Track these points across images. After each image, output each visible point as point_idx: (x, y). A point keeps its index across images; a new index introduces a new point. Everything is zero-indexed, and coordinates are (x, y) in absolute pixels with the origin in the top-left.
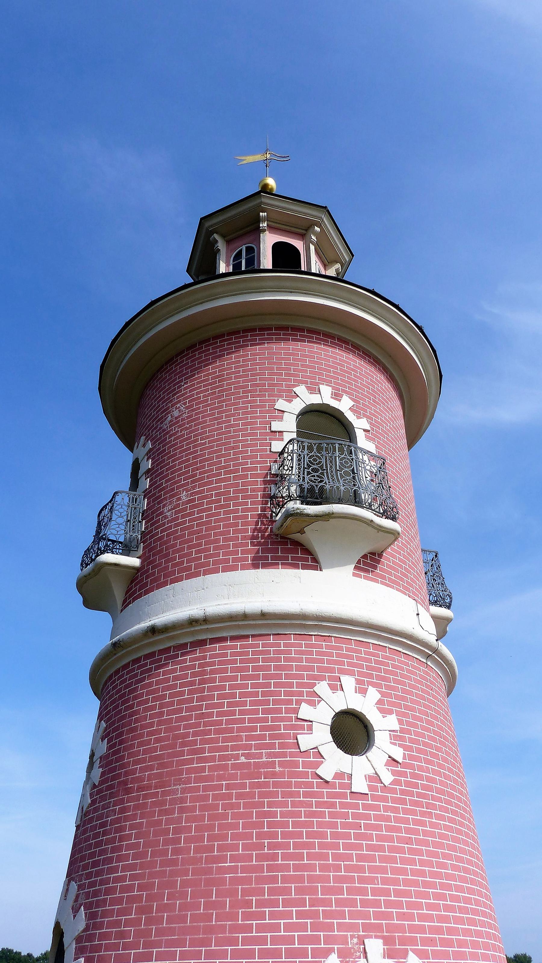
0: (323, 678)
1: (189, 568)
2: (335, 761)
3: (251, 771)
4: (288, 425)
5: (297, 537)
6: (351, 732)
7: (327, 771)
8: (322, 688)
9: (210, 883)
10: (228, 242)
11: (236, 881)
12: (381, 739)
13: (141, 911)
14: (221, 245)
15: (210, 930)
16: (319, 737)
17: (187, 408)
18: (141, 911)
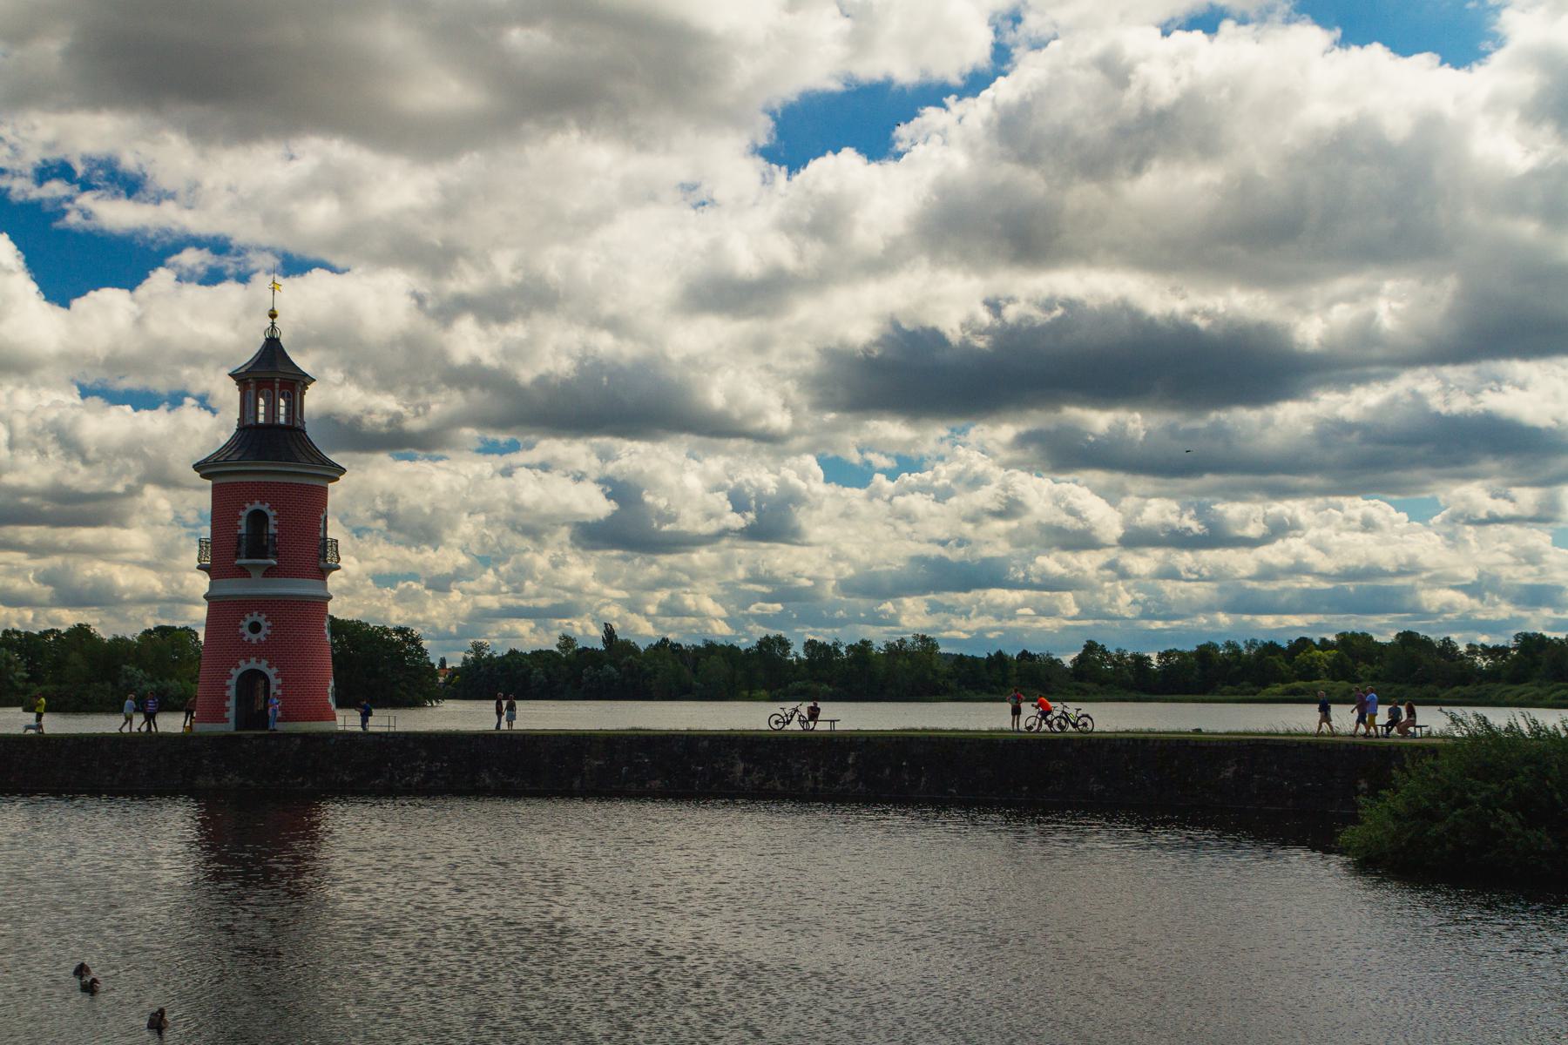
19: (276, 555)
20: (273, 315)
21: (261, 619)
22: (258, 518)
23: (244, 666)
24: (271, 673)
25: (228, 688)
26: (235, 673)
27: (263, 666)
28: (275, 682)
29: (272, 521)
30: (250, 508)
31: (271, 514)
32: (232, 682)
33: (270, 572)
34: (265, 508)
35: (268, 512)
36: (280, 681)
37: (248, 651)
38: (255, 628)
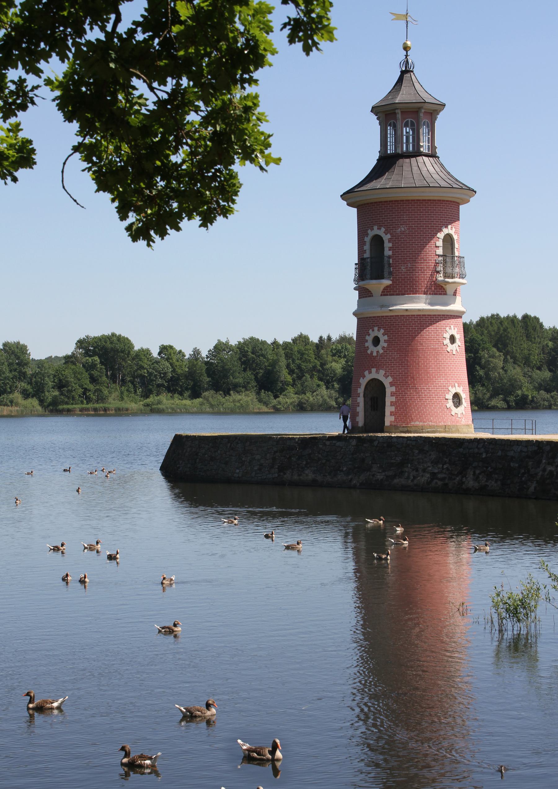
0: (447, 326)
1: (413, 291)
2: (450, 347)
3: (435, 349)
4: (440, 243)
5: (444, 286)
6: (453, 339)
7: (449, 349)
8: (447, 329)
9: (427, 373)
10: (402, 112)
11: (432, 373)
12: (457, 340)
13: (411, 378)
14: (399, 116)
15: (428, 382)
16: (447, 341)
17: (408, 229)
18: (411, 378)
19: (390, 273)
20: (406, 48)
21: (380, 334)
22: (378, 241)
23: (369, 376)
24: (387, 382)
25: (392, 394)
26: (363, 382)
27: (380, 376)
28: (389, 390)
29: (387, 245)
30: (371, 233)
31: (386, 238)
32: (361, 391)
33: (387, 291)
34: (381, 232)
35: (383, 235)
36: (393, 389)
37: (372, 362)
38: (376, 341)
